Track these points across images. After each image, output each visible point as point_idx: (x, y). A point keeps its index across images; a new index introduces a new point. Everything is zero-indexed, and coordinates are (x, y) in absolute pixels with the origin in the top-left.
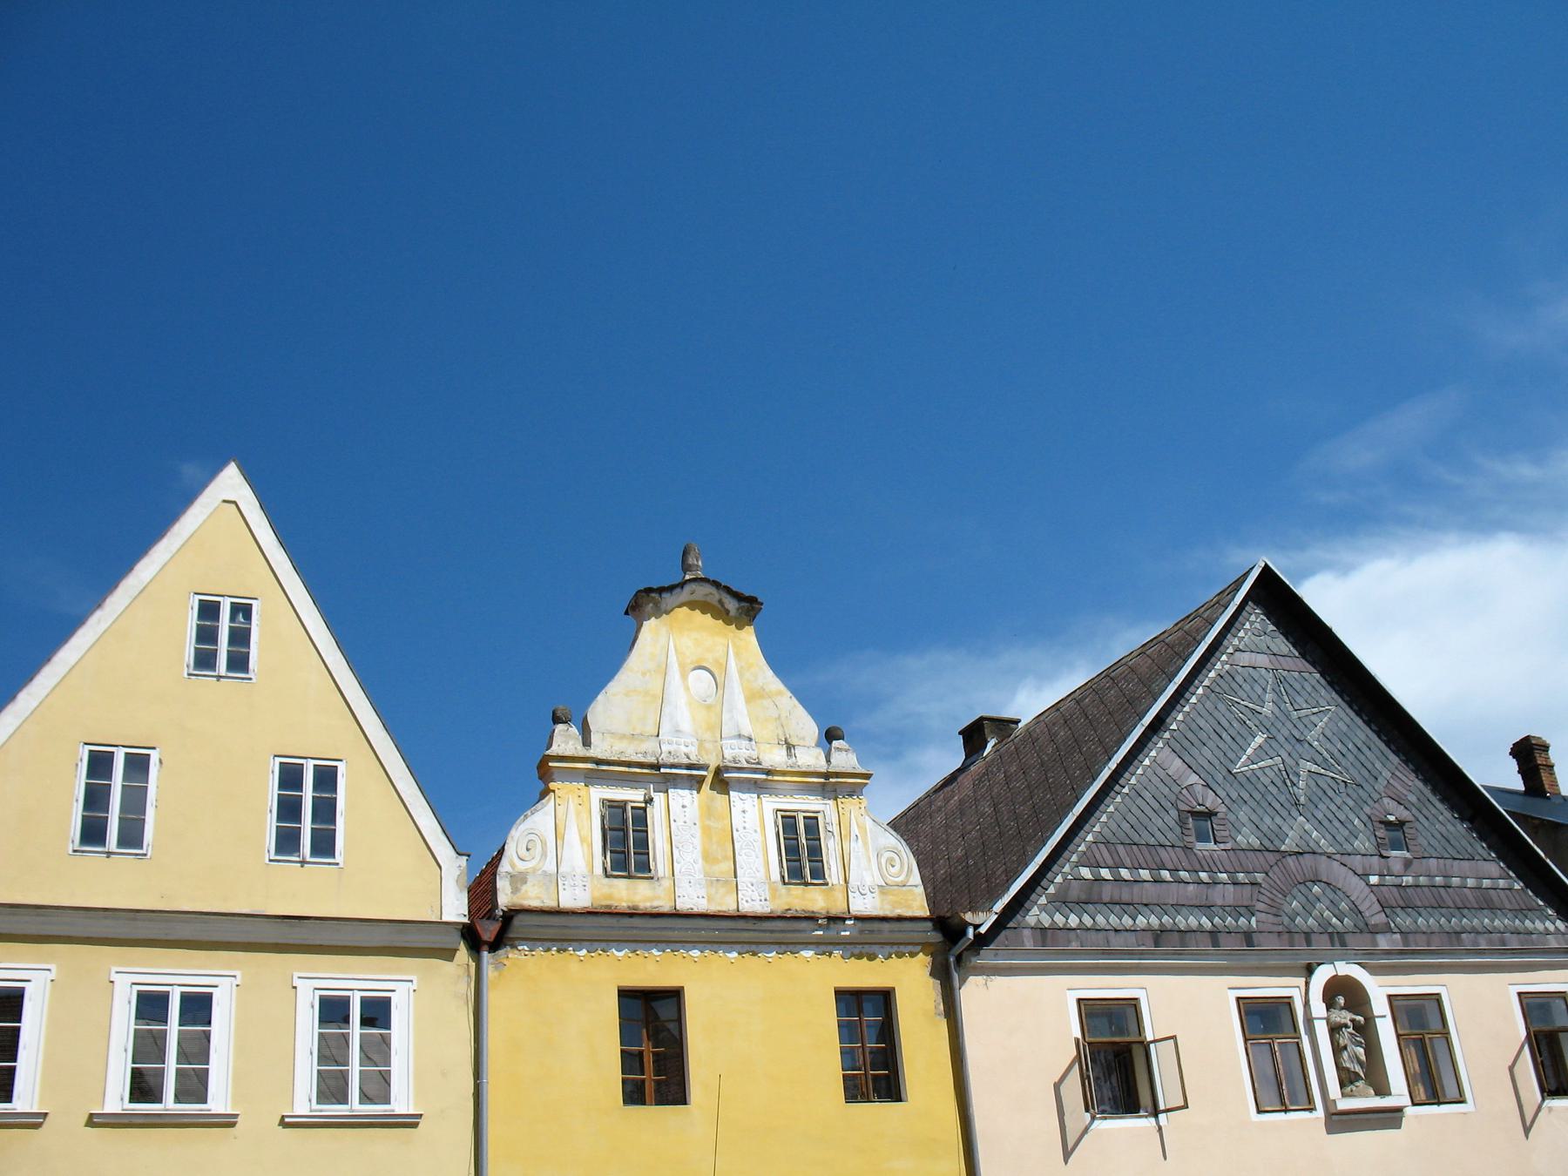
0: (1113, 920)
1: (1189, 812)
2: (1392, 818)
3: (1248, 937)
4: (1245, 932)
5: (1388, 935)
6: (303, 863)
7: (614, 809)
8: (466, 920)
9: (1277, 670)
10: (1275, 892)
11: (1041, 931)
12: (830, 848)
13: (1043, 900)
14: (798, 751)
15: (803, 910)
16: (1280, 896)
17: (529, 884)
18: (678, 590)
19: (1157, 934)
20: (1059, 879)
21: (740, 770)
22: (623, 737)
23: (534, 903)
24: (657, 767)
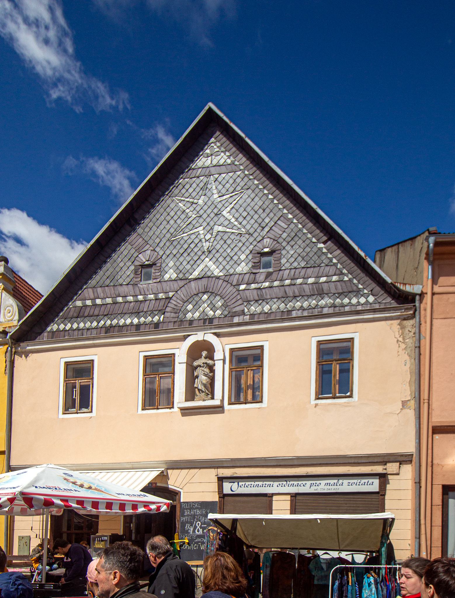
0: (88, 325)
1: (140, 265)
2: (266, 250)
3: (157, 325)
10: (178, 301)
11: (53, 332)
19: (108, 329)
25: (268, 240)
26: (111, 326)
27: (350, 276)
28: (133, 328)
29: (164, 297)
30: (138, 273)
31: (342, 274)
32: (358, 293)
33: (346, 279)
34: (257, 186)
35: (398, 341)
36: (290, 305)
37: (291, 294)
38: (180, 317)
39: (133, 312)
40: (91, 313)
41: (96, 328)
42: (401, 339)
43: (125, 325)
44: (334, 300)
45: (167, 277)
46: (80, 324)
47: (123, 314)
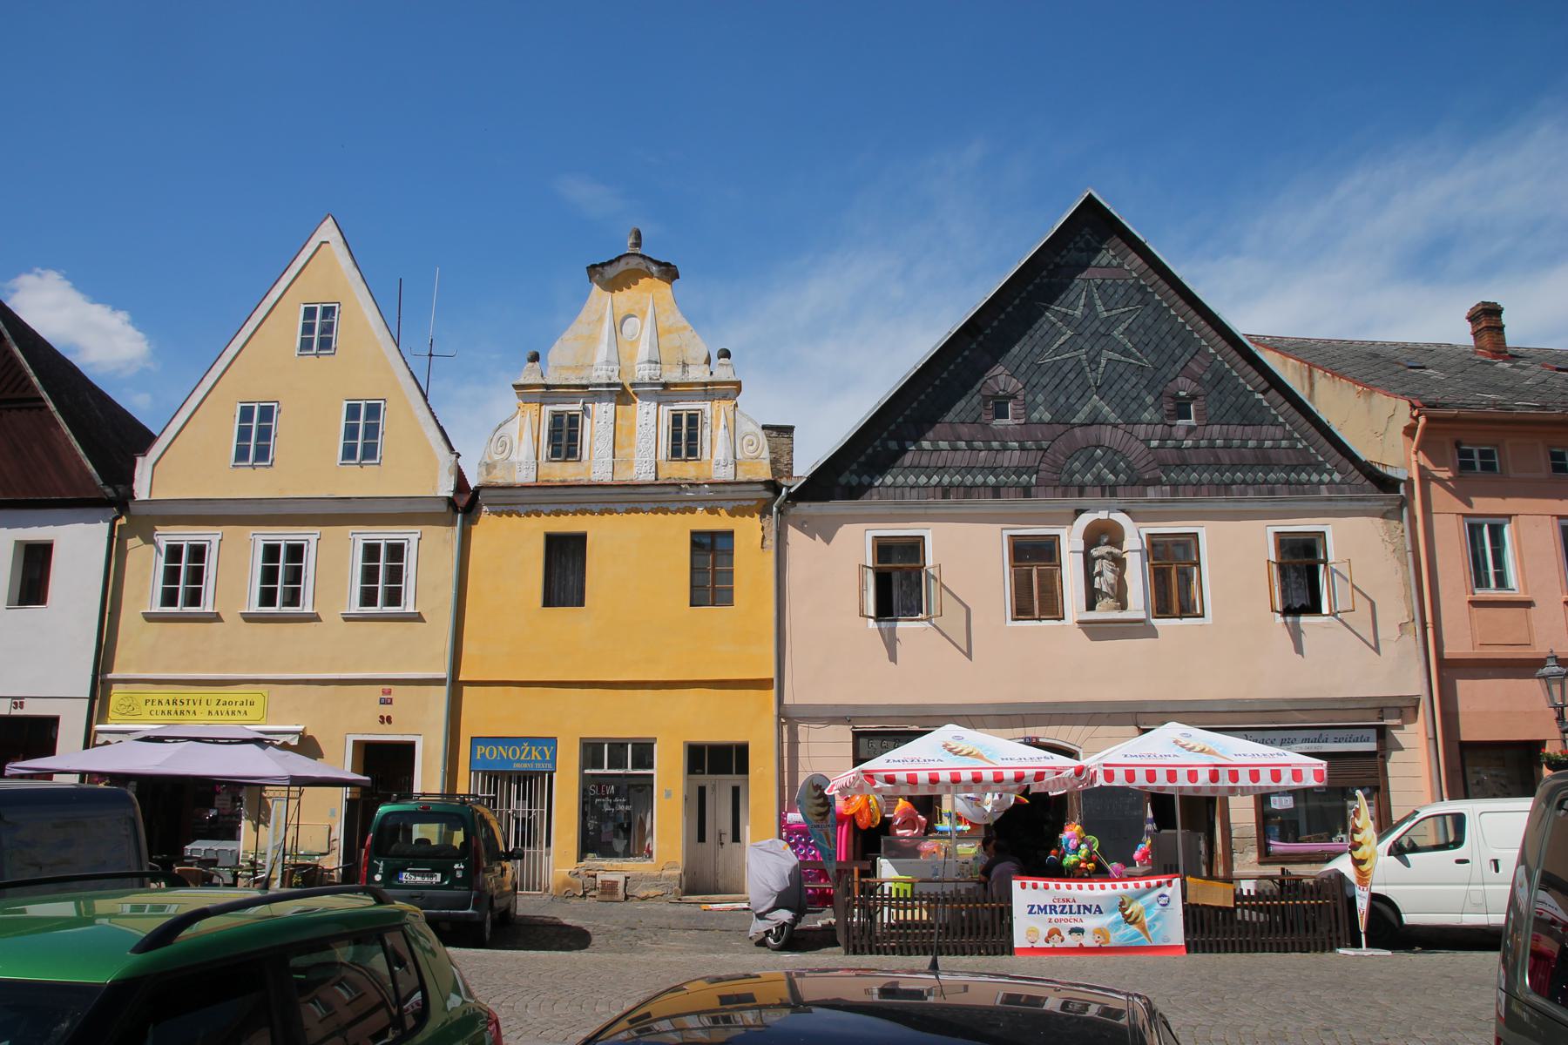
0: (912, 479)
1: (992, 396)
4: (1024, 487)
5: (1158, 487)
6: (359, 464)
7: (557, 418)
8: (451, 495)
9: (1093, 279)
12: (705, 435)
13: (854, 466)
14: (690, 369)
15: (680, 478)
16: (1062, 458)
17: (498, 469)
18: (616, 263)
20: (870, 451)
21: (644, 385)
22: (569, 368)
23: (501, 482)
24: (586, 387)
25: (1183, 379)
26: (951, 485)
27: (1305, 443)
28: (989, 491)
29: (1034, 447)
30: (988, 408)
31: (1291, 438)
32: (1318, 467)
33: (1300, 446)
34: (1160, 302)
35: (1383, 540)
36: (1227, 476)
37: (1227, 461)
38: (1063, 479)
39: (986, 466)
40: (916, 463)
41: (925, 486)
42: (1387, 538)
43: (974, 486)
44: (1288, 475)
45: (1035, 416)
46: (898, 478)
47: (969, 469)
